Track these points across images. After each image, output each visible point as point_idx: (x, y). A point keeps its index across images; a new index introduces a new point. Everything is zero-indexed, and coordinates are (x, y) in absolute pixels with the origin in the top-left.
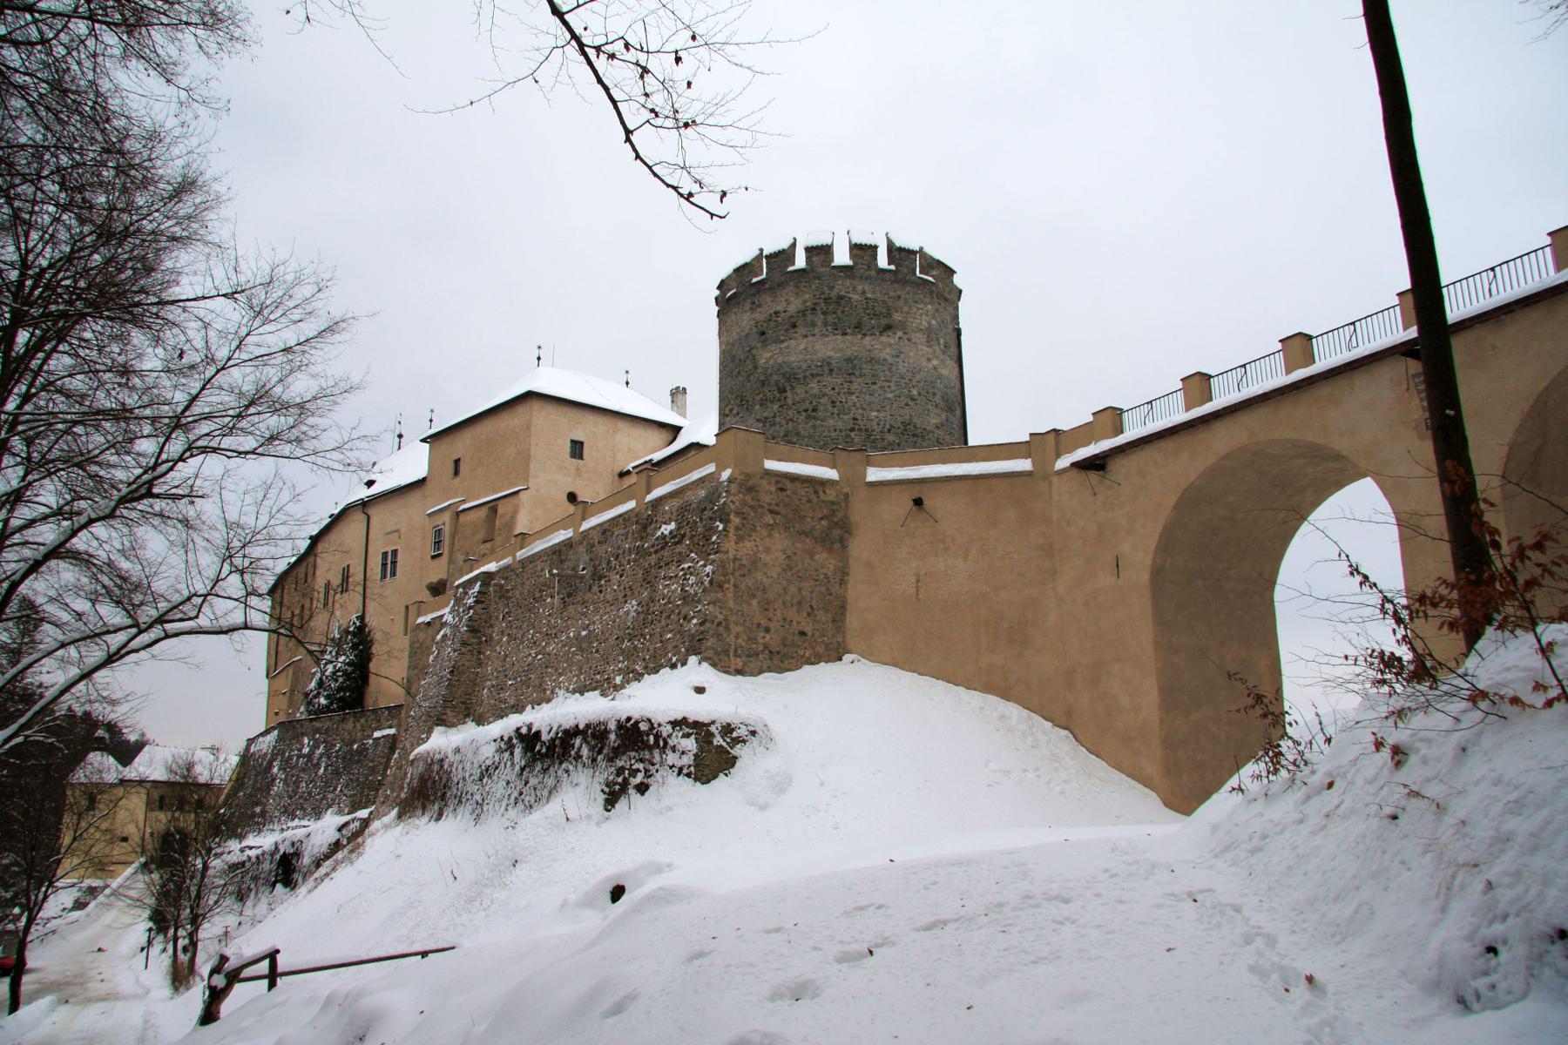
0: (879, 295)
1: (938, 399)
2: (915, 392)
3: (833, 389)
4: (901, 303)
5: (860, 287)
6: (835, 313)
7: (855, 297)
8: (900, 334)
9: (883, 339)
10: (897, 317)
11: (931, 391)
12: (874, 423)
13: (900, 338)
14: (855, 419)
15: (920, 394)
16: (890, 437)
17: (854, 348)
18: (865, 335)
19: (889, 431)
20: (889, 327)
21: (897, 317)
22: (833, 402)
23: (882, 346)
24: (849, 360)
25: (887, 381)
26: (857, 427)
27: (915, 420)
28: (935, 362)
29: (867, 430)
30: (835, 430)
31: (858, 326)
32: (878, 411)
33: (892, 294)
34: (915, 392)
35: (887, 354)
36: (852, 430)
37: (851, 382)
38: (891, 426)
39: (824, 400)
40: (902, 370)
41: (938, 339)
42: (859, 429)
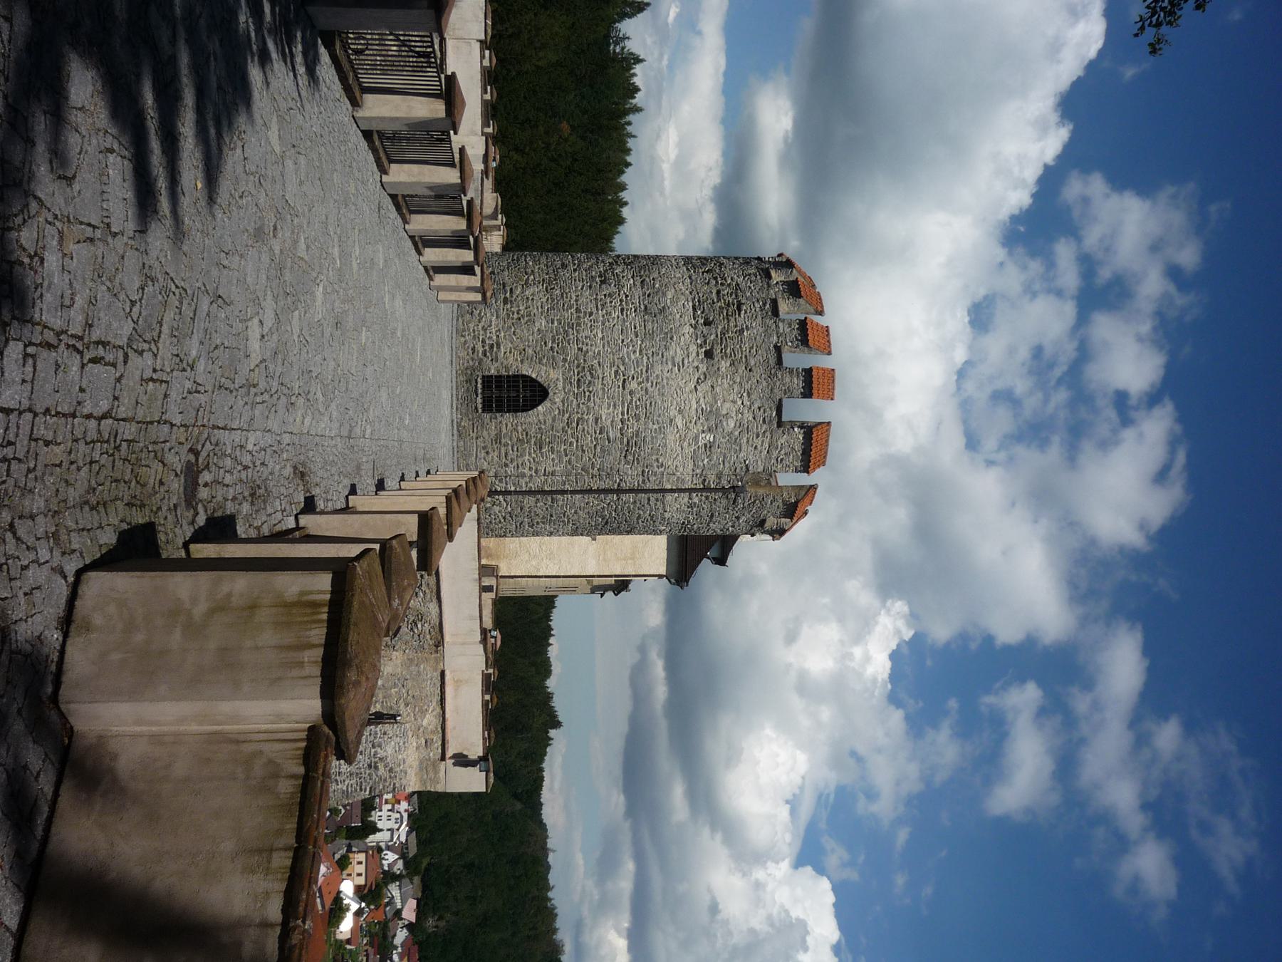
1: (633, 427)
2: (634, 385)
3: (627, 296)
5: (754, 325)
6: (719, 300)
7: (741, 320)
8: (703, 368)
9: (693, 348)
12: (587, 333)
13: (697, 367)
14: (591, 314)
15: (631, 393)
16: (573, 350)
17: (678, 316)
18: (695, 328)
19: (580, 349)
20: (709, 354)
21: (724, 365)
22: (610, 295)
23: (685, 343)
24: (662, 310)
25: (641, 351)
26: (582, 315)
28: (679, 422)
29: (578, 325)
30: (577, 296)
31: (707, 323)
32: (603, 338)
33: (752, 363)
34: (634, 385)
35: (676, 351)
36: (578, 310)
37: (635, 311)
38: (587, 352)
39: (613, 289)
40: (658, 369)
41: (709, 430)
42: (579, 317)
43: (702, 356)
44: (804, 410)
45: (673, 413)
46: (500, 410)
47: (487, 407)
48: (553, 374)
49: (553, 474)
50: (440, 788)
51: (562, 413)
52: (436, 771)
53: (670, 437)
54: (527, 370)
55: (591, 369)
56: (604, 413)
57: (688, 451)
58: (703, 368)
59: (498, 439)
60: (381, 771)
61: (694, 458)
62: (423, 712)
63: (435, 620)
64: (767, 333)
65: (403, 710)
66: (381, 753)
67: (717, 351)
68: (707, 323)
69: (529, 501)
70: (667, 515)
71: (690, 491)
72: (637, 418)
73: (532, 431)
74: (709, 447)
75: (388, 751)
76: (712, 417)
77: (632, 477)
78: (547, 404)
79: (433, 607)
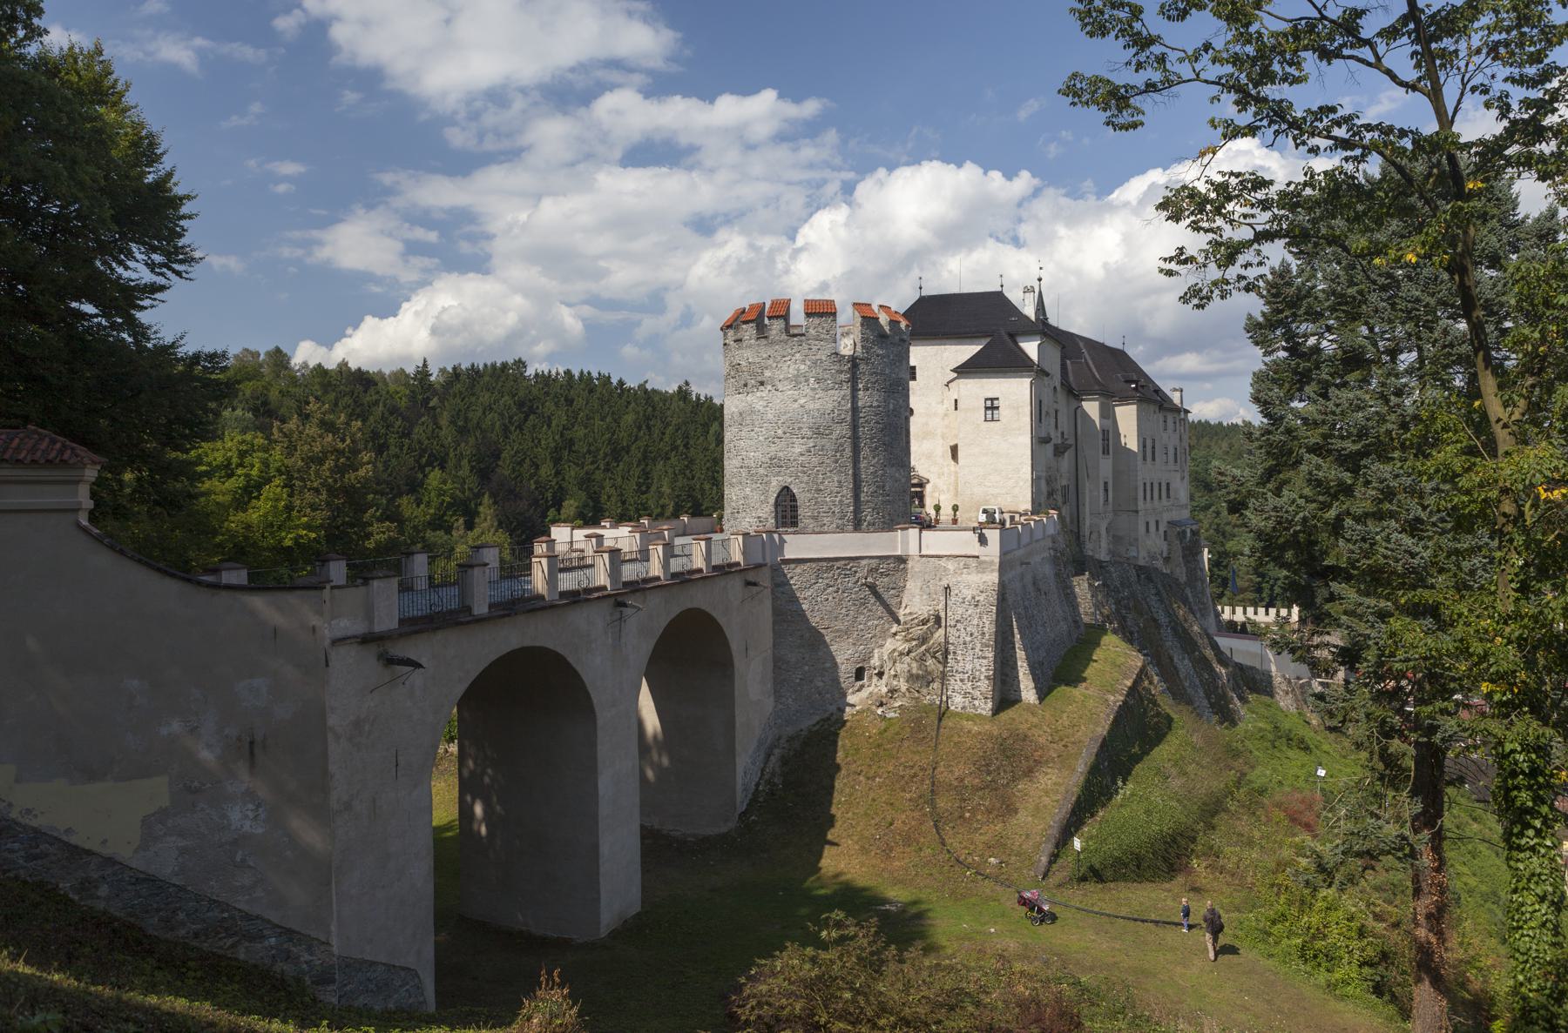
0: (757, 360)
2: (780, 432)
4: (770, 362)
8: (769, 387)
9: (759, 394)
10: (767, 373)
11: (796, 427)
16: (761, 471)
20: (762, 383)
21: (767, 373)
27: (781, 454)
28: (802, 401)
31: (746, 385)
35: (759, 406)
40: (770, 416)
41: (807, 381)
43: (762, 388)
44: (797, 316)
45: (796, 405)
46: (796, 517)
47: (795, 524)
48: (774, 483)
49: (840, 482)
50: (997, 560)
51: (797, 477)
52: (985, 562)
53: (812, 407)
54: (772, 500)
55: (771, 459)
56: (797, 450)
57: (821, 394)
58: (769, 387)
59: (815, 518)
60: (981, 598)
61: (826, 390)
62: (946, 569)
63: (877, 561)
64: (750, 346)
65: (945, 583)
66: (969, 597)
67: (760, 379)
68: (746, 385)
69: (863, 497)
70: (875, 404)
71: (854, 390)
72: (800, 428)
73: (810, 496)
74: (818, 381)
75: (968, 593)
76: (797, 380)
77: (843, 430)
78: (792, 487)
79: (864, 562)
